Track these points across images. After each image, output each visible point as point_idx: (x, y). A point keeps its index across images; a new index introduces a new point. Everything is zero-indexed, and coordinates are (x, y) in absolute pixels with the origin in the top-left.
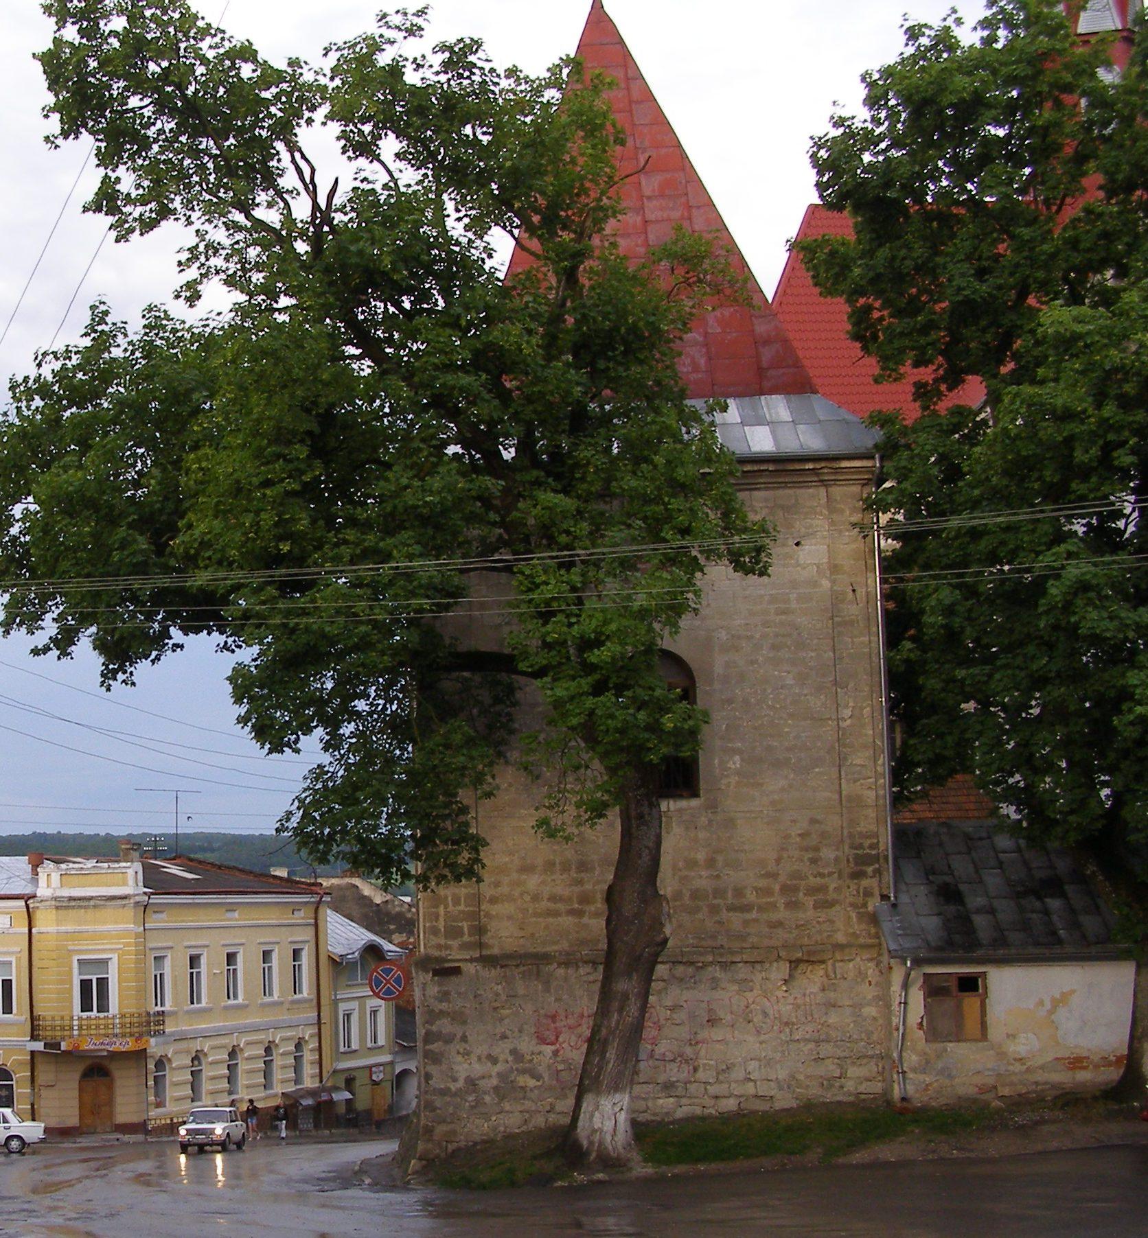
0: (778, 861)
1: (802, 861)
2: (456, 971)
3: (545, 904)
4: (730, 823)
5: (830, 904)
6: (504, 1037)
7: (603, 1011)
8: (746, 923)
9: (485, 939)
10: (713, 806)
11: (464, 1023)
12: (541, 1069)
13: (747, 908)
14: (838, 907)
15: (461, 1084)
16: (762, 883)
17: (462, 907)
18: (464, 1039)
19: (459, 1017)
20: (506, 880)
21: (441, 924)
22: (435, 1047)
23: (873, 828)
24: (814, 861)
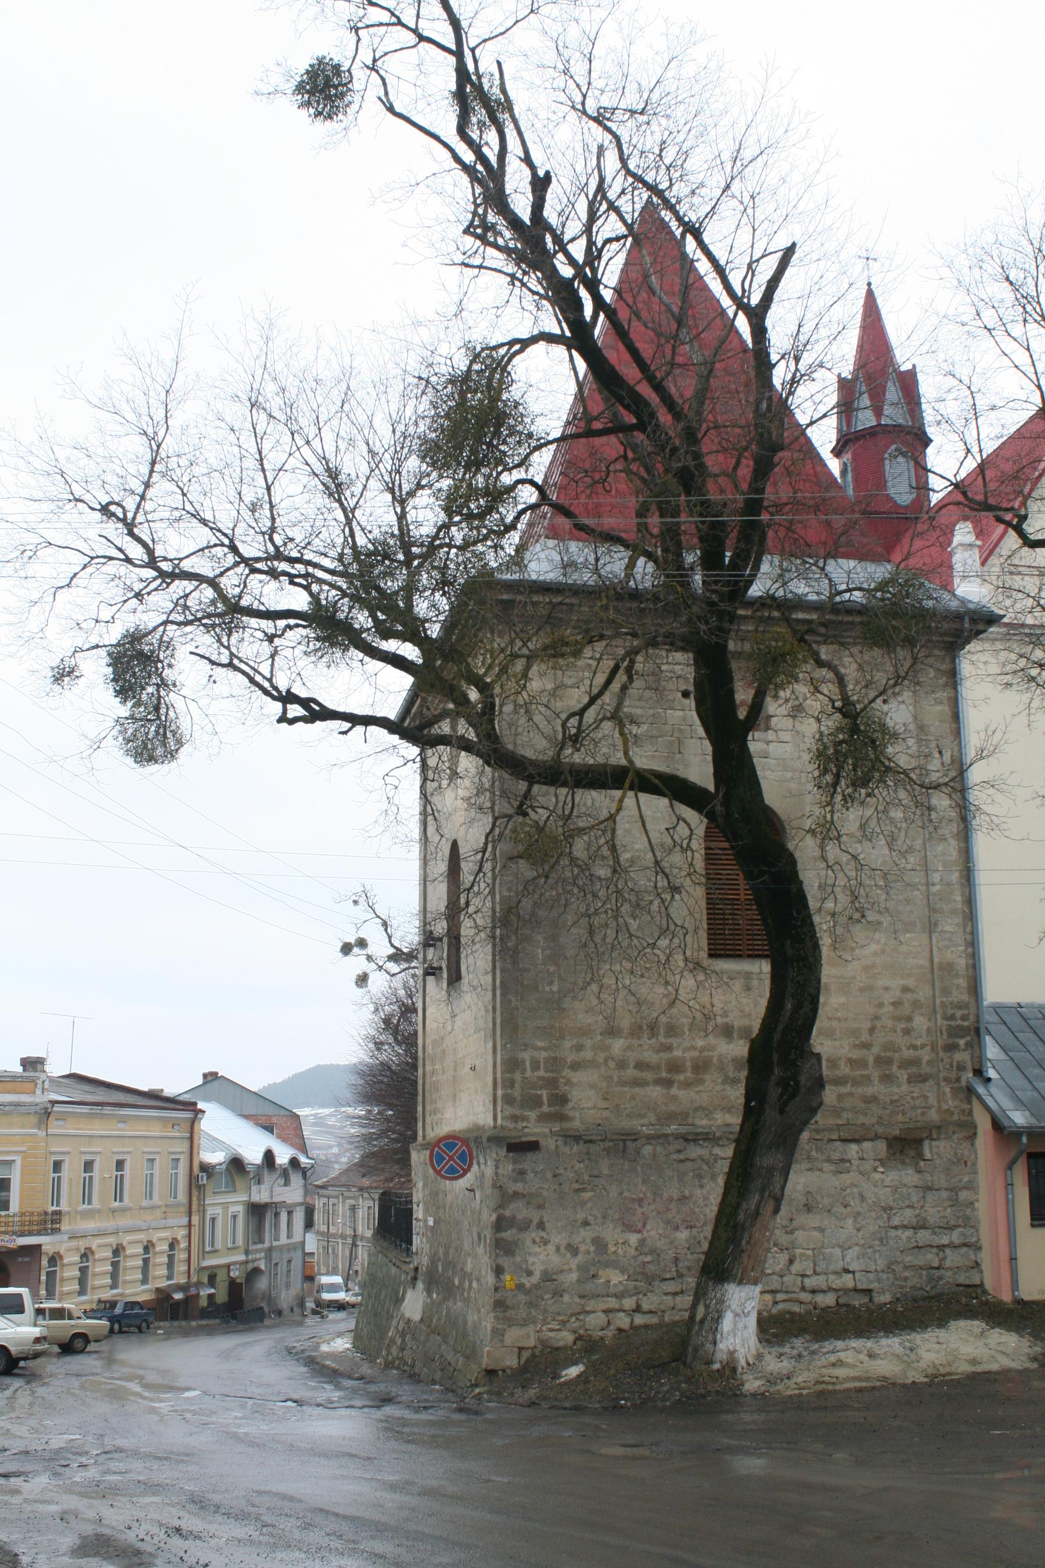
0: (872, 1030)
1: (895, 1031)
2: (533, 1146)
3: (631, 1072)
6: (586, 1223)
9: (567, 1110)
11: (541, 1207)
14: (931, 1082)
15: (535, 1279)
16: (856, 1054)
17: (541, 1073)
18: (541, 1226)
20: (588, 1043)
21: (517, 1093)
22: (507, 1235)
23: (965, 997)
24: (907, 1032)
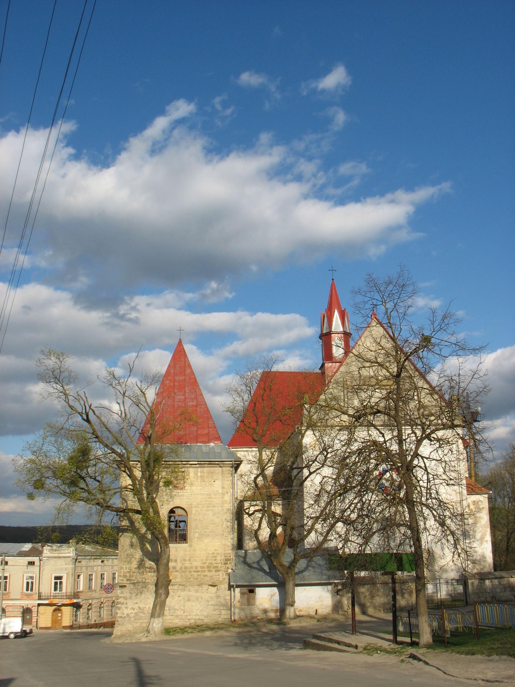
0: (206, 560)
2: (125, 586)
4: (195, 550)
5: (219, 571)
6: (136, 603)
7: (156, 598)
8: (198, 575)
10: (190, 546)
11: (127, 599)
12: (145, 612)
13: (198, 572)
16: (202, 565)
18: (126, 604)
19: (125, 598)
